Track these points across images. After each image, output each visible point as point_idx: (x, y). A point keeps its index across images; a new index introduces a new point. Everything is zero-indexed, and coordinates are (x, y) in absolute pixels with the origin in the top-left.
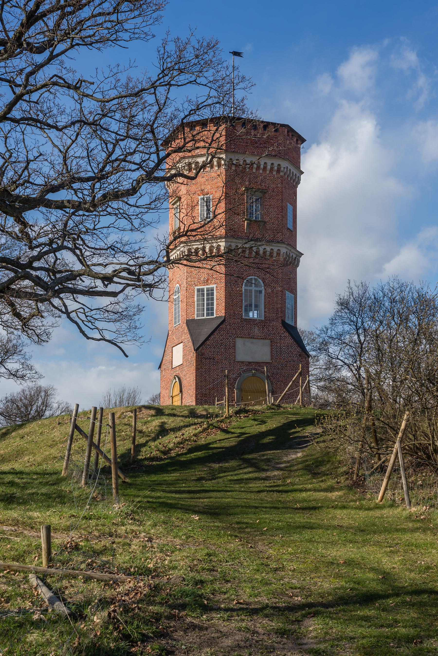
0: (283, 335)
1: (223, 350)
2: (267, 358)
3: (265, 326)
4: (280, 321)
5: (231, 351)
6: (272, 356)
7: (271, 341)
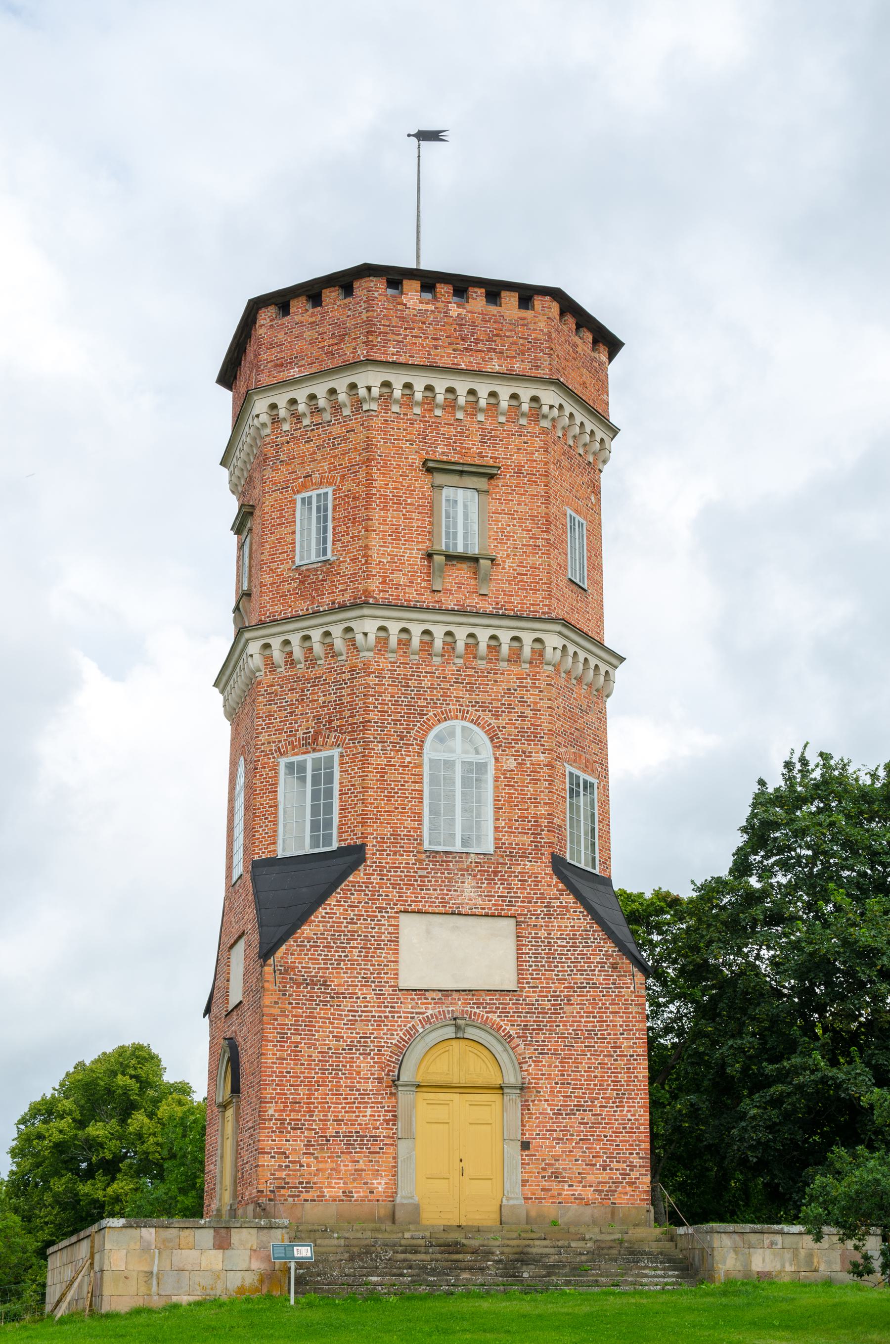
0: (556, 903)
1: (355, 952)
2: (510, 983)
3: (496, 873)
4: (547, 859)
5: (385, 955)
6: (520, 971)
7: (518, 924)
